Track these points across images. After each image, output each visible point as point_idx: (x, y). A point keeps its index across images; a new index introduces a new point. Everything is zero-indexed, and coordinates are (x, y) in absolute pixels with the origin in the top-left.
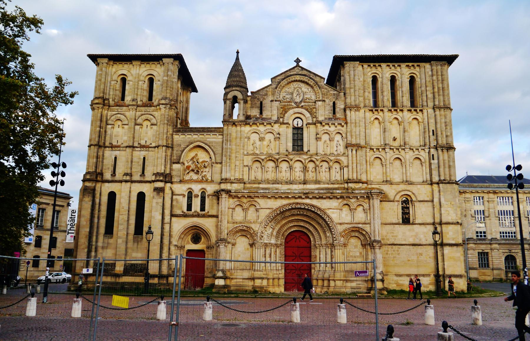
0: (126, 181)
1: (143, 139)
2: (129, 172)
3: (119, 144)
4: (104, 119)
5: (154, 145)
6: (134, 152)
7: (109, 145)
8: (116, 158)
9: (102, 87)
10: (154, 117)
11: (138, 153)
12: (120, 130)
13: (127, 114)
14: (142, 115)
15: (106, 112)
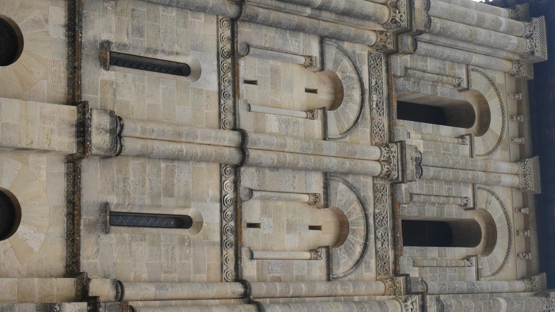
0: (82, 130)
1: (265, 212)
2: (129, 145)
3: (243, 87)
4: (346, 29)
5: (250, 270)
6: (215, 169)
7: (241, 38)
8: (182, 70)
9: (461, 28)
10: (358, 263)
11: (214, 192)
12: (300, 98)
13: (364, 133)
14: (362, 203)
15: (373, 38)
